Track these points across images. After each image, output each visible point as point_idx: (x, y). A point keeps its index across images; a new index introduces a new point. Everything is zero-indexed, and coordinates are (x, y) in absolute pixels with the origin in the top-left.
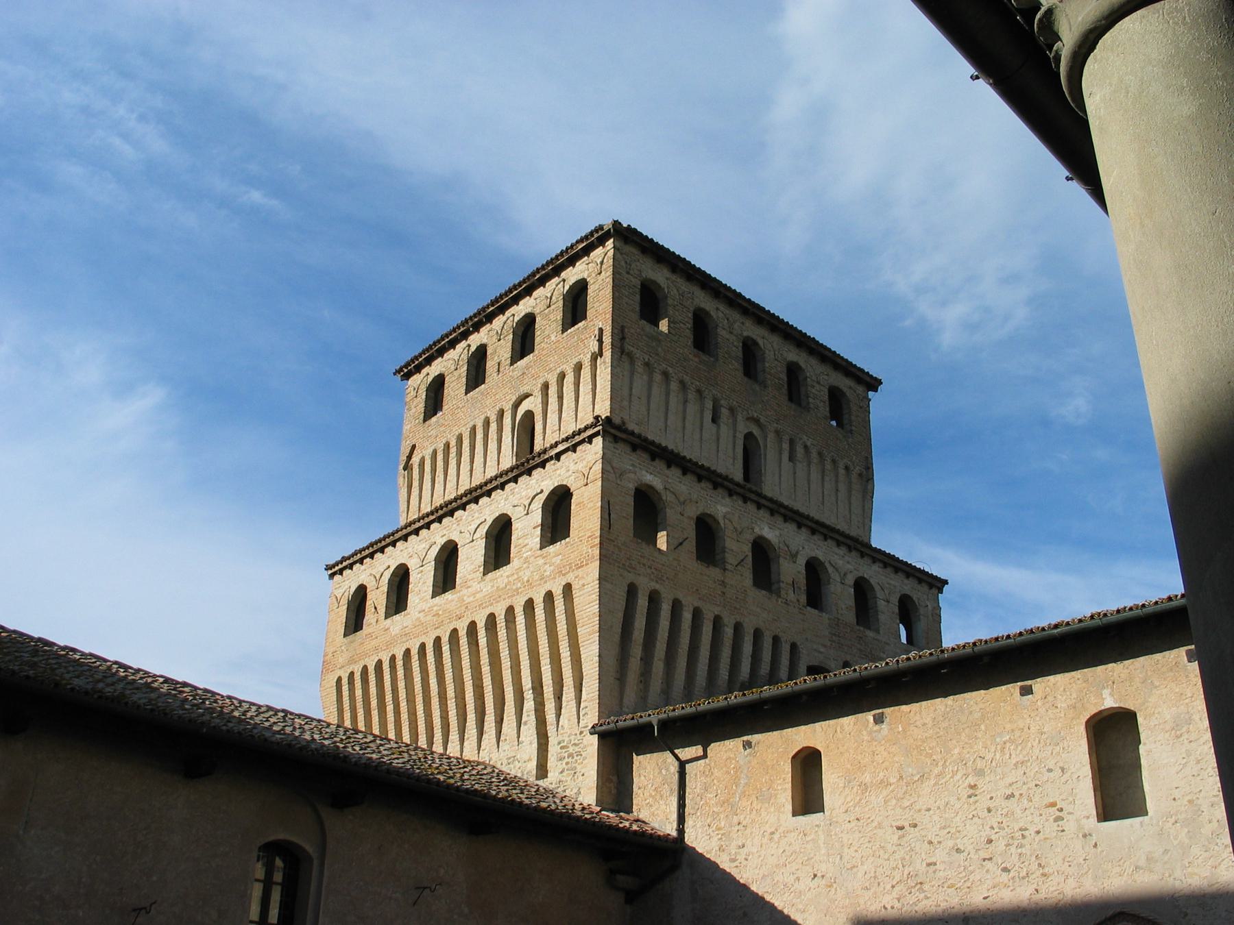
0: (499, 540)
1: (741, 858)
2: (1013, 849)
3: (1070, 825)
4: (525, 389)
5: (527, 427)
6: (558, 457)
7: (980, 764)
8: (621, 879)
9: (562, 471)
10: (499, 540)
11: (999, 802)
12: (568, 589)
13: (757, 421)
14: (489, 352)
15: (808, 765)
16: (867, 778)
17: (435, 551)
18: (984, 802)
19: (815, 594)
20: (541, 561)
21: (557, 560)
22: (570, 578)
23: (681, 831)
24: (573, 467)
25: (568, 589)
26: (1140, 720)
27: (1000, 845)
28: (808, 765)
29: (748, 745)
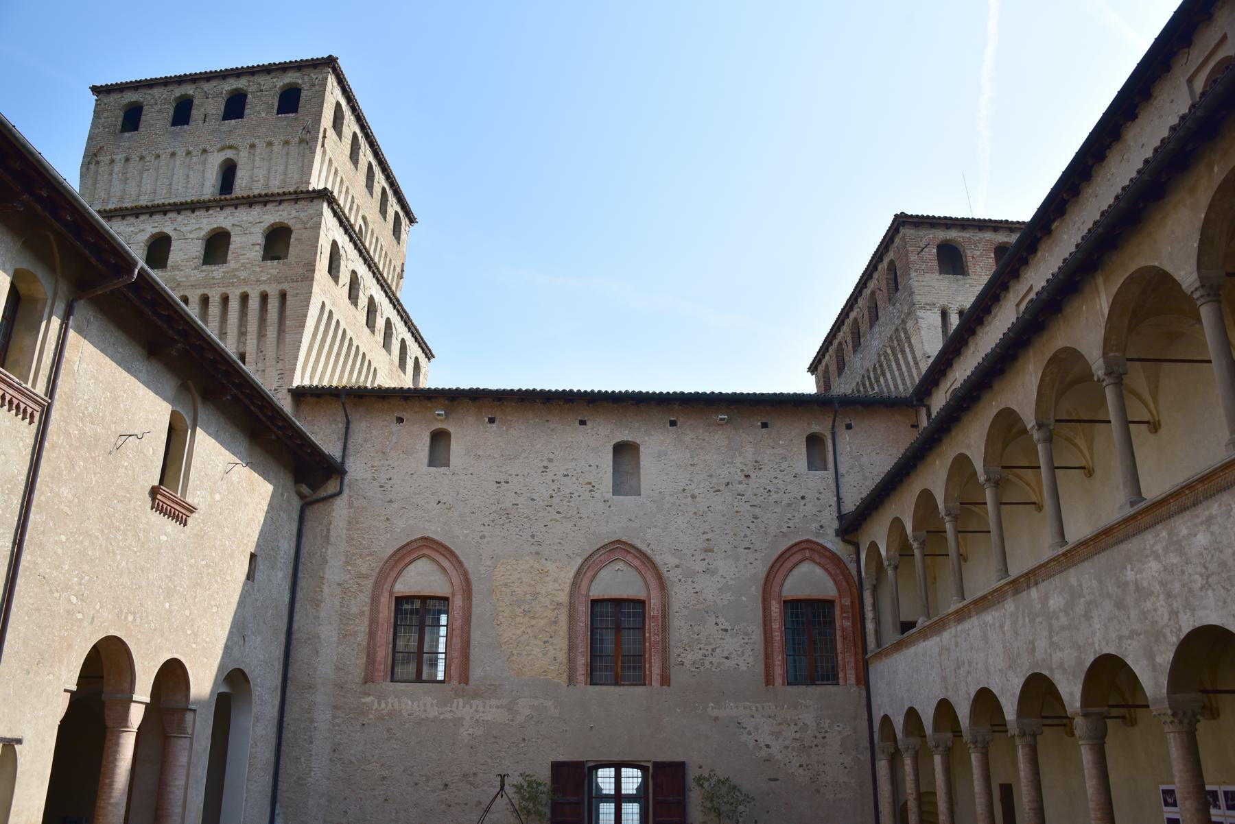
0: (216, 247)
1: (388, 486)
2: (565, 503)
3: (597, 494)
4: (227, 142)
5: (229, 172)
6: (280, 202)
7: (551, 456)
8: (305, 489)
9: (285, 213)
10: (216, 247)
11: (560, 477)
12: (283, 296)
13: (364, 218)
14: (196, 102)
15: (439, 439)
16: (480, 452)
17: (145, 236)
18: (550, 476)
19: (386, 345)
20: (258, 269)
21: (275, 272)
22: (285, 286)
23: (343, 462)
24: (294, 213)
25: (283, 296)
26: (642, 449)
27: (556, 500)
28: (439, 439)
29: (400, 420)
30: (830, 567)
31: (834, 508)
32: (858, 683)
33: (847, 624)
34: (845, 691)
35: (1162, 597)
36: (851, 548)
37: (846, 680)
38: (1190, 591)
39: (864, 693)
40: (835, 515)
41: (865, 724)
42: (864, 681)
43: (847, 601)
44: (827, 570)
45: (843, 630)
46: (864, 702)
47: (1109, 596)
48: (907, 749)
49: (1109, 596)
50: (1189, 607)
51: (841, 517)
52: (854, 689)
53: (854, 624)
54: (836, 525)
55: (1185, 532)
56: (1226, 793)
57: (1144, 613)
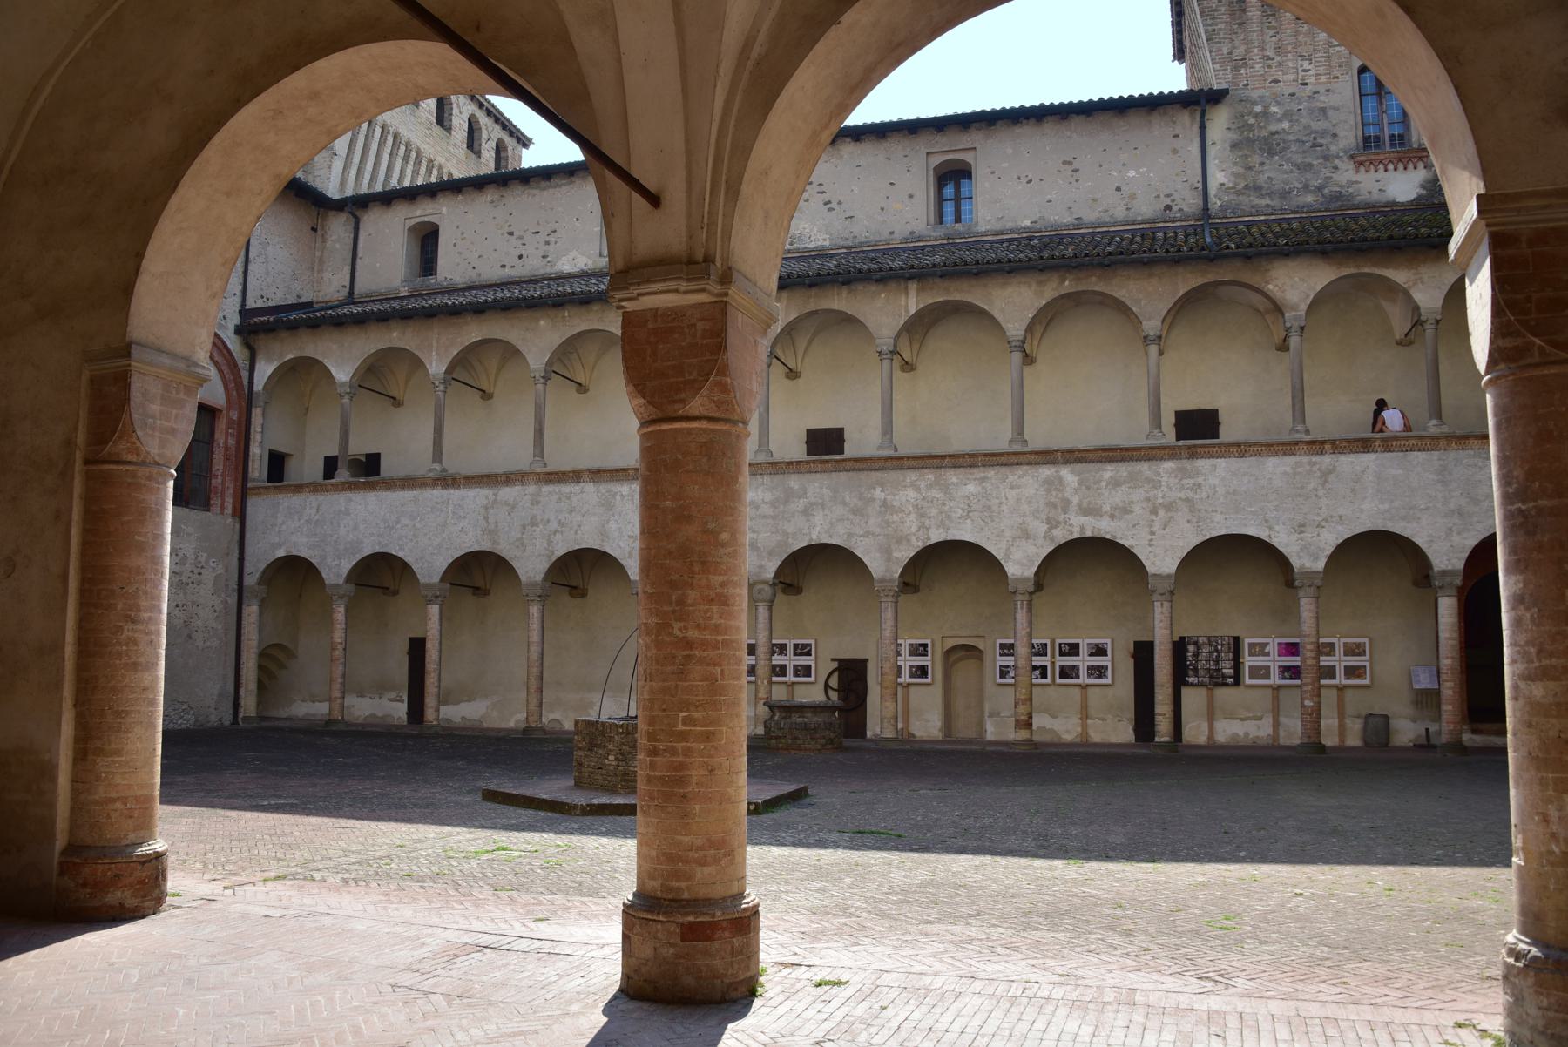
30: (225, 369)
31: (238, 299)
32: (233, 515)
33: (232, 442)
34: (220, 521)
35: (913, 516)
36: (247, 353)
37: (222, 507)
38: (948, 517)
39: (238, 526)
40: (238, 308)
41: (235, 562)
42: (241, 514)
43: (234, 415)
44: (221, 372)
45: (227, 448)
46: (237, 537)
47: (844, 504)
48: (341, 597)
49: (844, 504)
50: (942, 525)
51: (244, 312)
52: (230, 520)
53: (238, 443)
54: (236, 320)
55: (954, 480)
56: (796, 646)
57: (888, 523)
